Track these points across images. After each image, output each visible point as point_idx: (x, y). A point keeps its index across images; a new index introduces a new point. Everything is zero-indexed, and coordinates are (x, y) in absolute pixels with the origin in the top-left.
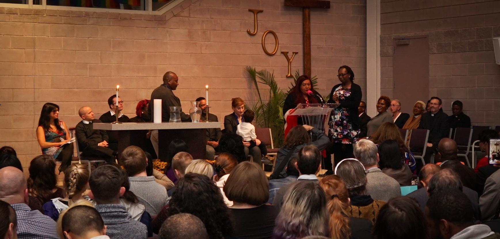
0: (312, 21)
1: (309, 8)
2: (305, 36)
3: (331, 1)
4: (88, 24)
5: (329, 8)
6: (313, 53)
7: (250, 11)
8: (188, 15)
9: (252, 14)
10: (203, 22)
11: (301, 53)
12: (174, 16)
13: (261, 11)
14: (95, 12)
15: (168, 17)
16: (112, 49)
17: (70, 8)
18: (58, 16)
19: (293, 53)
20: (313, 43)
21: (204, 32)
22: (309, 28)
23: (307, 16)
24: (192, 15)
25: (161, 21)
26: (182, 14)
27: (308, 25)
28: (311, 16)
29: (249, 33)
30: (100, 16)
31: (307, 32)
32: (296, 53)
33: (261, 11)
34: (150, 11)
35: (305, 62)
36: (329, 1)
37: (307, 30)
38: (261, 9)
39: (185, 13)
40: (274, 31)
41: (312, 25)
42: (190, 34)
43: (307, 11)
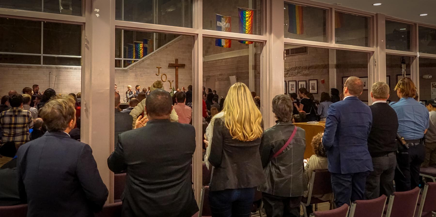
1: (178, 66)
7: (157, 67)
8: (135, 69)
9: (158, 69)
10: (140, 71)
12: (131, 69)
13: (161, 68)
15: (128, 70)
20: (179, 77)
21: (141, 74)
22: (178, 73)
24: (136, 69)
25: (126, 71)
26: (133, 69)
28: (178, 69)
29: (156, 75)
33: (161, 68)
34: (123, 68)
37: (177, 73)
38: (161, 67)
39: (134, 68)
40: (166, 74)
42: (136, 75)
43: (177, 68)
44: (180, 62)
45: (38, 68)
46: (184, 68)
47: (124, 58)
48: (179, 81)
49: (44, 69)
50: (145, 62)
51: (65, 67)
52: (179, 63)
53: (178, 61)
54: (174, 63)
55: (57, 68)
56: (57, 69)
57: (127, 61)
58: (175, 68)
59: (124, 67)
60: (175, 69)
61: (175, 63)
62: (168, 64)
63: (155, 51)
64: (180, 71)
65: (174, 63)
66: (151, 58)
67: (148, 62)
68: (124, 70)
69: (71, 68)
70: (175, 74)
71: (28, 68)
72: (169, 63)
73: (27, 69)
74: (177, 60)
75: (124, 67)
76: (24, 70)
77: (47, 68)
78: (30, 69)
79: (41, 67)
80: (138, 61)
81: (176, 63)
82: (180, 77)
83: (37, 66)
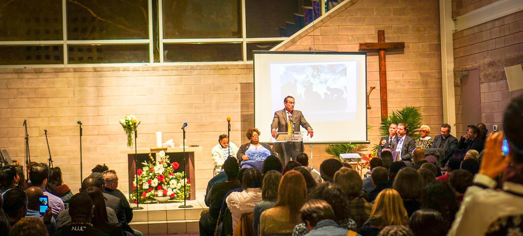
0: (387, 60)
1: (384, 49)
2: (381, 72)
3: (405, 42)
4: (193, 74)
6: (389, 87)
11: (378, 87)
14: (199, 65)
16: (212, 92)
17: (182, 63)
18: (170, 70)
19: (371, 88)
22: (385, 66)
23: (383, 57)
28: (386, 56)
30: (201, 68)
31: (383, 69)
32: (374, 88)
35: (382, 95)
36: (404, 42)
37: (383, 68)
43: (382, 53)
44: (390, 38)
45: (57, 71)
46: (404, 53)
48: (390, 86)
49: (68, 74)
50: (298, 43)
51: (113, 67)
52: (387, 41)
53: (385, 35)
55: (95, 70)
56: (95, 72)
58: (377, 53)
60: (378, 56)
61: (377, 42)
62: (359, 45)
63: (325, 14)
64: (391, 60)
66: (312, 34)
67: (305, 44)
69: (114, 70)
70: (378, 70)
71: (36, 74)
72: (362, 42)
73: (35, 76)
74: (381, 34)
76: (29, 79)
77: (75, 70)
78: (41, 76)
79: (62, 71)
81: (378, 41)
82: (391, 76)
83: (54, 68)
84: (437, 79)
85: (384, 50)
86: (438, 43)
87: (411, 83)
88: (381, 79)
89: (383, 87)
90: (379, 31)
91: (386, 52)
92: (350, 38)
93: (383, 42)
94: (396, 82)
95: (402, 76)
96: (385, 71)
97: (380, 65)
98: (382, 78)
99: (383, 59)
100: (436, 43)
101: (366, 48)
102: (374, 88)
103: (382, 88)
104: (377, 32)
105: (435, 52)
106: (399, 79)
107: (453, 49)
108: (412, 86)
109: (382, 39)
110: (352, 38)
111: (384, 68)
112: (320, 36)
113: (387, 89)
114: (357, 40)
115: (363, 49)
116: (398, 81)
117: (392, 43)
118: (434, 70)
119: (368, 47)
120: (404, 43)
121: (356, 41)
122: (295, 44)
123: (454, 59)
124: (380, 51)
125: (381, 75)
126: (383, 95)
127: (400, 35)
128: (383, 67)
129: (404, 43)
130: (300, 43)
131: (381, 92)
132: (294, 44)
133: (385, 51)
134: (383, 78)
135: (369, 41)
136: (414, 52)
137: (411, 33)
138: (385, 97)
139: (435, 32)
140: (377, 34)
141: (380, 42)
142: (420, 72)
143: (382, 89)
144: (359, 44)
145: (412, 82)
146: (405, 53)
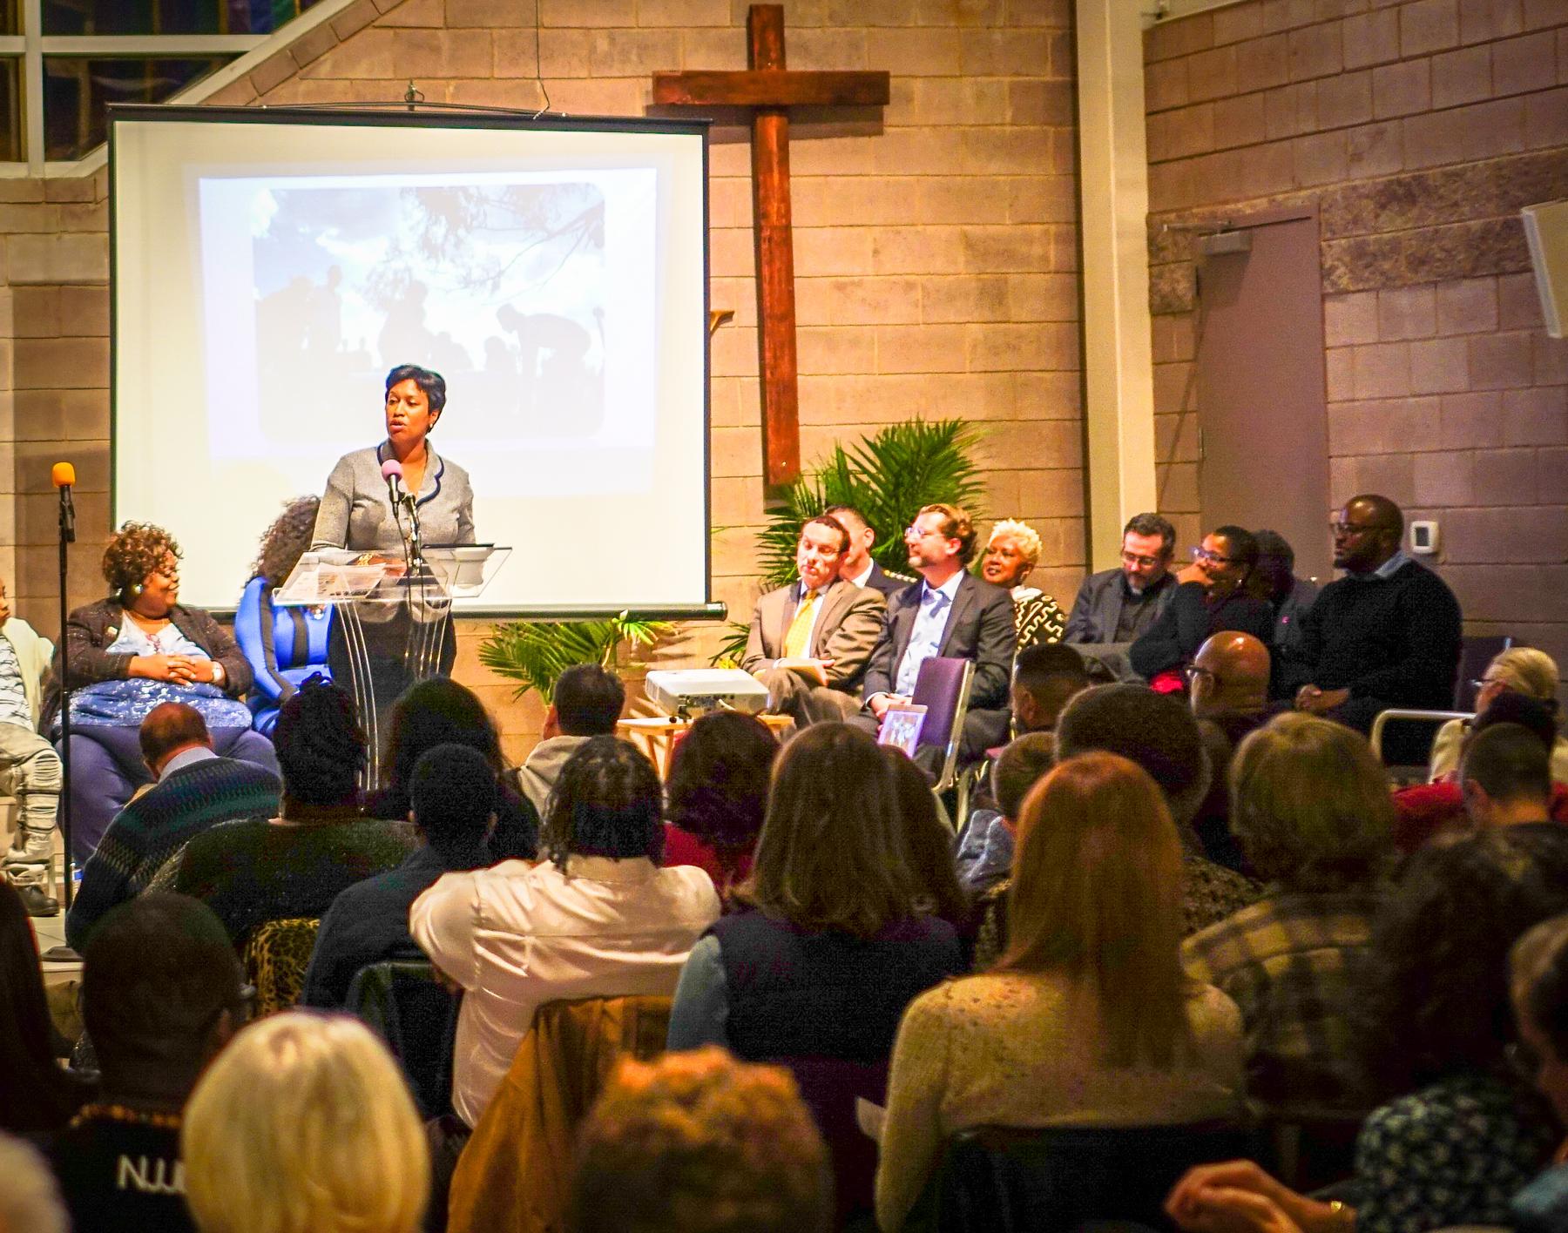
0: (795, 166)
1: (780, 109)
2: (766, 233)
3: (892, 74)
5: (884, 99)
6: (803, 314)
20: (803, 263)
22: (785, 200)
23: (775, 148)
27: (781, 180)
28: (793, 144)
32: (727, 316)
35: (768, 355)
37: (774, 207)
41: (800, 185)
43: (772, 126)
47: (46, 31)
52: (795, 64)
53: (787, 32)
54: (737, 63)
57: (98, 65)
58: (743, 130)
59: (50, 155)
60: (747, 147)
61: (742, 66)
62: (649, 84)
65: (737, 63)
68: (50, 196)
72: (664, 67)
75: (61, 142)
80: (234, 56)
84: (1057, 272)
85: (780, 116)
86: (1061, 79)
87: (918, 294)
88: (766, 271)
89: (778, 311)
90: (753, 11)
91: (790, 122)
92: (603, 45)
93: (775, 68)
94: (840, 287)
95: (871, 254)
96: (787, 228)
97: (762, 192)
98: (771, 263)
99: (775, 160)
100: (1049, 78)
101: (689, 100)
102: (727, 316)
103: (770, 317)
104: (744, 12)
105: (1045, 128)
106: (858, 270)
107: (1148, 114)
108: (924, 307)
109: (773, 55)
110: (612, 41)
111: (779, 208)
112: (440, 33)
113: (798, 322)
114: (639, 56)
115: (673, 104)
116: (853, 283)
117: (822, 76)
118: (1038, 228)
119: (700, 97)
120: (885, 76)
121: (634, 58)
122: (309, 73)
123: (1151, 164)
124: (759, 120)
125: (765, 246)
126: (775, 357)
127: (864, 31)
128: (776, 205)
129: (885, 76)
130: (335, 66)
131: (767, 340)
132: (301, 73)
133: (785, 120)
134: (778, 264)
135: (699, 62)
136: (935, 126)
137: (921, 23)
138: (785, 367)
139: (1044, 23)
140: (744, 23)
141: (761, 67)
142: (965, 235)
143: (768, 324)
144: (650, 81)
145: (924, 288)
146: (888, 130)
